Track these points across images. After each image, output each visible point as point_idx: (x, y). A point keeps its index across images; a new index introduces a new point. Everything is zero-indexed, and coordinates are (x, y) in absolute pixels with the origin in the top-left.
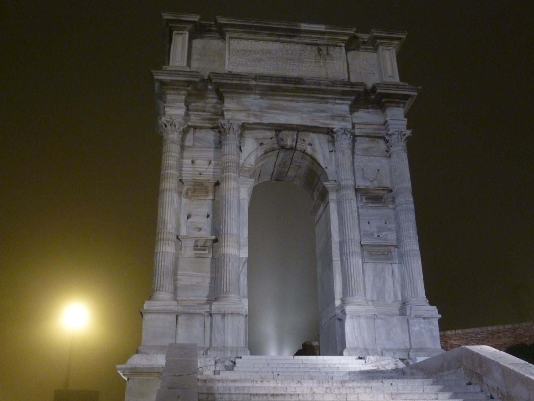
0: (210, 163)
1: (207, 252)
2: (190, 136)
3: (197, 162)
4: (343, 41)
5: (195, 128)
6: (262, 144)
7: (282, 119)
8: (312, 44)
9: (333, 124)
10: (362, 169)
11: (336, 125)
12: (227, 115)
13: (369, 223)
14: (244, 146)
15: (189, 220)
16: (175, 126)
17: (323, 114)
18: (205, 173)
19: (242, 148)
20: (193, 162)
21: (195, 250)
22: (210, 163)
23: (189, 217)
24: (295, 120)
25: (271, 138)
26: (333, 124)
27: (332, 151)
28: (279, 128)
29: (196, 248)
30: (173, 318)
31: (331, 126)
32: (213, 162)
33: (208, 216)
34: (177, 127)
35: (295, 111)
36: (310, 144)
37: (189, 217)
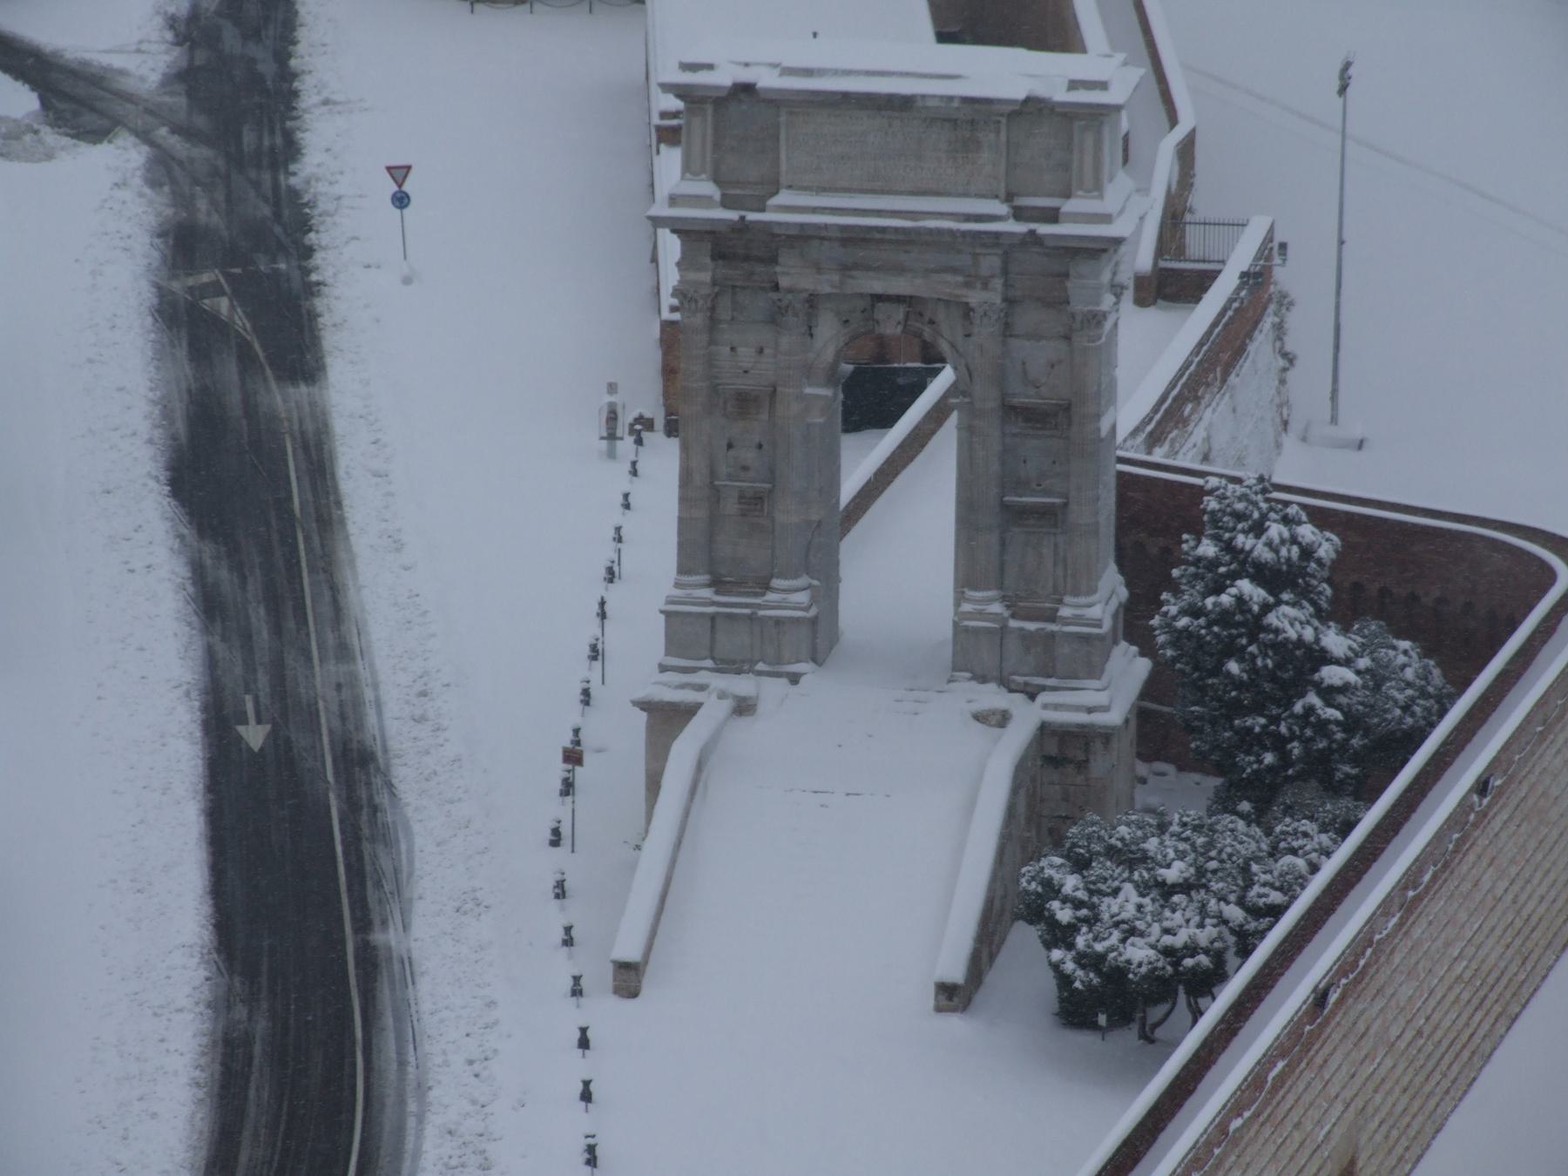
0: (761, 351)
1: (759, 507)
2: (725, 302)
3: (741, 350)
4: (1002, 115)
5: (734, 287)
6: (847, 321)
7: (878, 285)
8: (945, 120)
9: (966, 296)
10: (1024, 364)
11: (975, 297)
12: (784, 282)
13: (1025, 462)
14: (816, 326)
15: (732, 453)
16: (696, 302)
17: (949, 277)
18: (752, 371)
19: (814, 331)
20: (733, 349)
21: (740, 503)
22: (761, 351)
23: (730, 446)
24: (900, 286)
25: (863, 312)
26: (966, 296)
27: (968, 336)
28: (879, 298)
29: (743, 501)
30: (709, 624)
31: (965, 300)
32: (767, 351)
33: (760, 446)
34: (701, 302)
35: (900, 270)
36: (932, 322)
37: (730, 446)
